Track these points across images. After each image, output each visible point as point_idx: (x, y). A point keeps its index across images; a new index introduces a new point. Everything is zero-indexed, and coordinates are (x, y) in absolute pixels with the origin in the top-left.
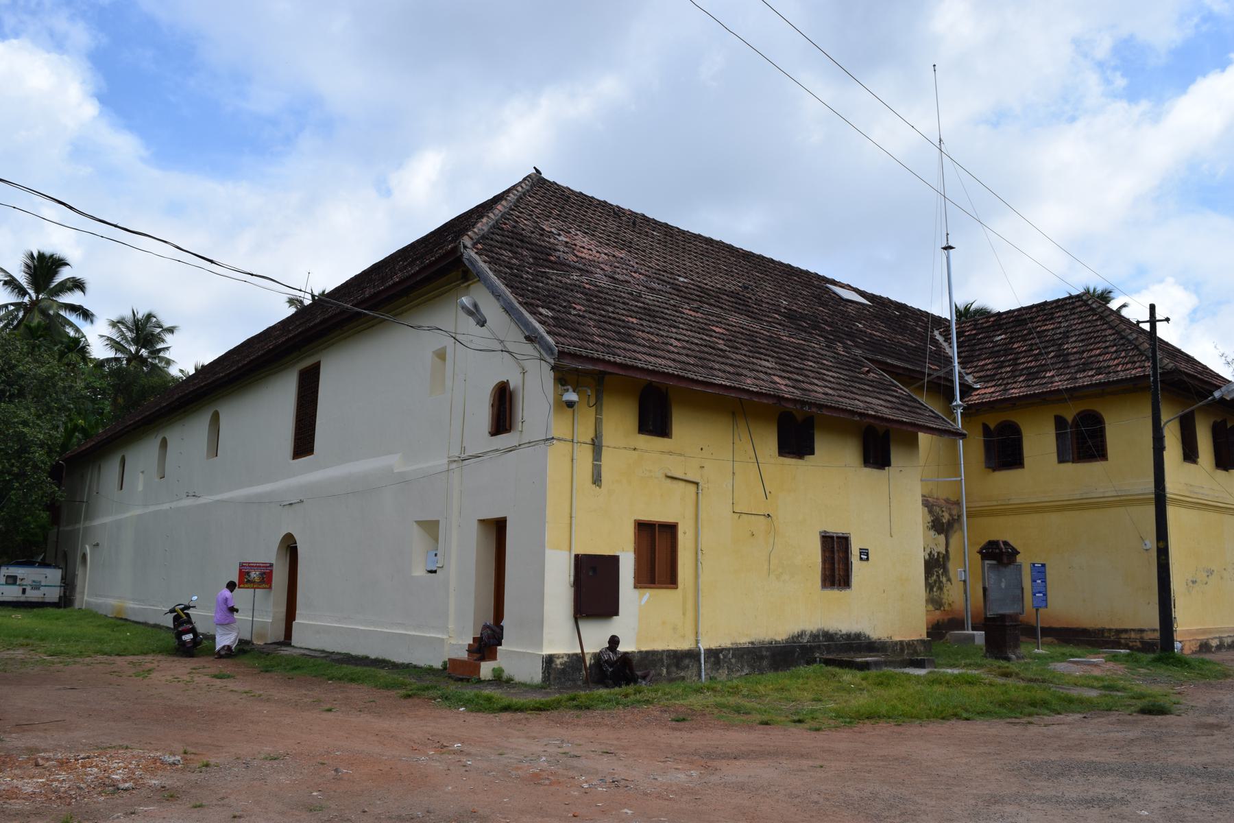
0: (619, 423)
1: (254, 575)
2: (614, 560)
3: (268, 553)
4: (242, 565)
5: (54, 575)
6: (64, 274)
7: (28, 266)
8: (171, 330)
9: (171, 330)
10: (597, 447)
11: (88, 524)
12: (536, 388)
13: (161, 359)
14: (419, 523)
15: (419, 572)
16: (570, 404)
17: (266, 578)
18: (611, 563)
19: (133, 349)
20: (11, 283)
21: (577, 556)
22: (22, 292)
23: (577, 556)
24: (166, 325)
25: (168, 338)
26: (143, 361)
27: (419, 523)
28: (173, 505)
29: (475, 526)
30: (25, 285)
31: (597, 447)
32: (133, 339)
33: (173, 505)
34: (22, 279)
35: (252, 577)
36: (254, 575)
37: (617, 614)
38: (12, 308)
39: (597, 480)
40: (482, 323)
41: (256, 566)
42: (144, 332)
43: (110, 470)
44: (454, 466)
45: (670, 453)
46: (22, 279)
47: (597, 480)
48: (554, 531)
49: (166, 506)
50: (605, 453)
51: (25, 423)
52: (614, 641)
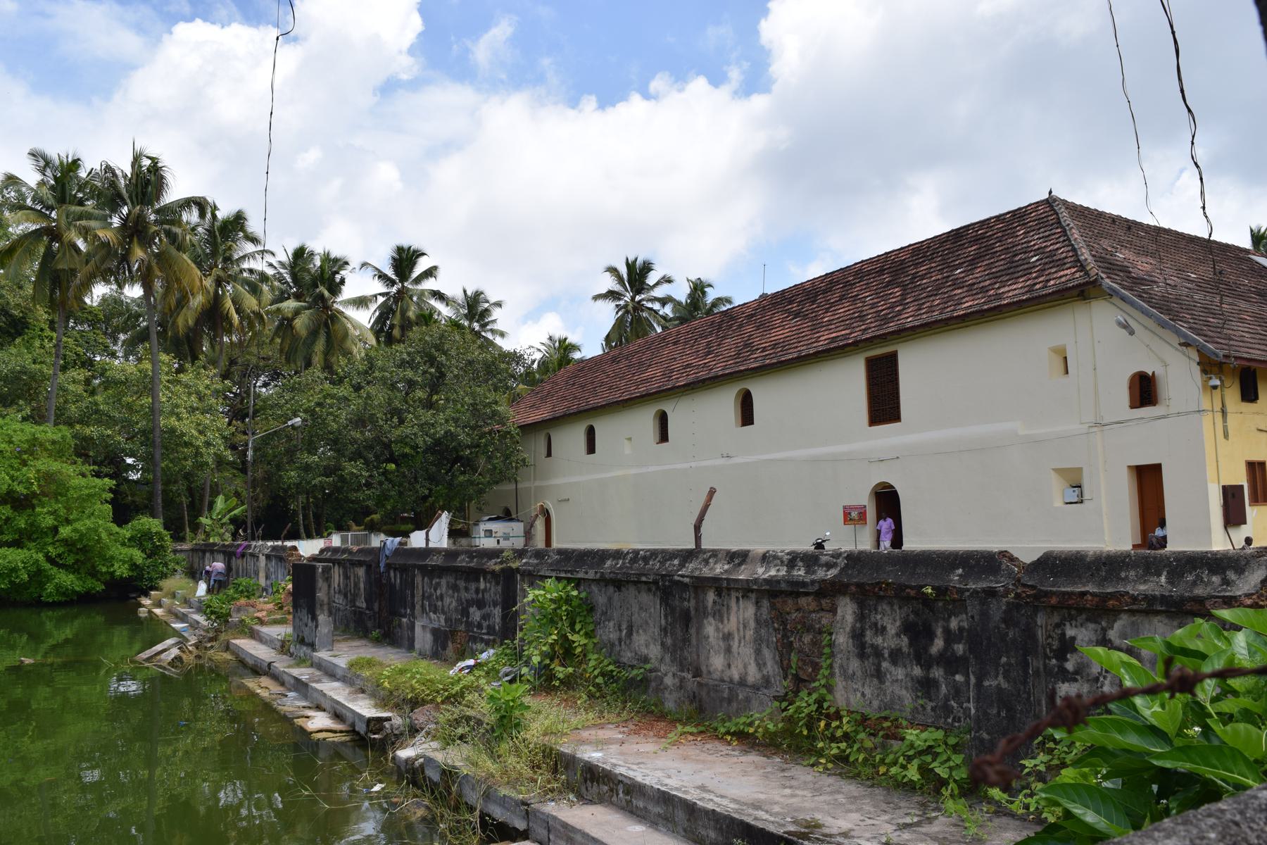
0: (1233, 394)
1: (854, 514)
2: (1242, 486)
3: (864, 498)
4: (845, 508)
5: (517, 528)
6: (422, 265)
7: (393, 258)
8: (499, 304)
9: (499, 304)
10: (1224, 412)
11: (537, 483)
12: (1180, 377)
13: (492, 331)
14: (1055, 470)
15: (1058, 503)
16: (1215, 387)
17: (862, 516)
18: (1242, 486)
19: (466, 324)
20: (382, 277)
21: (1224, 487)
22: (393, 283)
23: (1224, 487)
24: (492, 300)
25: (496, 314)
26: (478, 334)
27: (1055, 470)
28: (693, 464)
29: (1126, 469)
30: (394, 277)
31: (1224, 412)
32: (466, 315)
33: (693, 464)
34: (390, 273)
35: (853, 516)
36: (854, 514)
37: (1245, 523)
38: (381, 300)
39: (1226, 436)
40: (1132, 333)
41: (855, 508)
42: (476, 307)
43: (570, 440)
44: (1095, 429)
45: (1258, 413)
46: (390, 273)
47: (1226, 436)
48: (1211, 473)
49: (678, 466)
50: (1229, 417)
51: (496, 403)
52: (1248, 541)
